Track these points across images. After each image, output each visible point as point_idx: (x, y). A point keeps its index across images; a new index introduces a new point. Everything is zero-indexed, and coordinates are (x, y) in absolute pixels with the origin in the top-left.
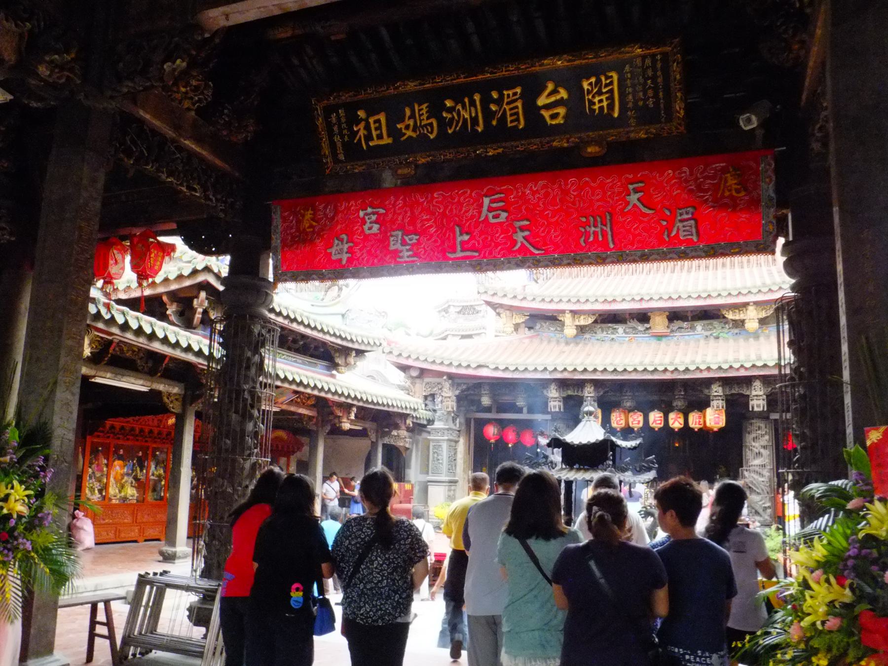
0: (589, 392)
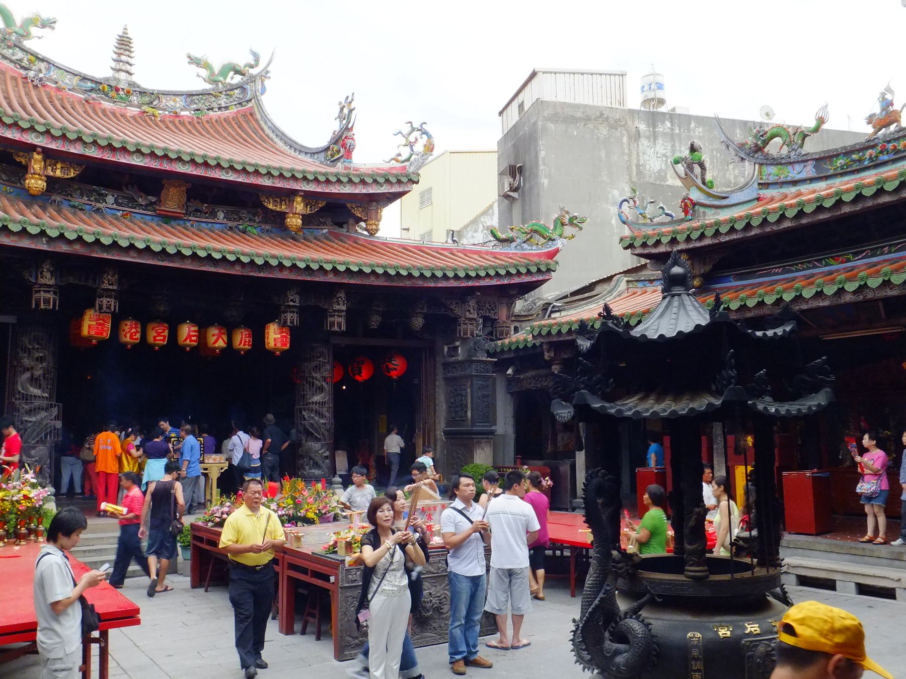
0: (109, 282)
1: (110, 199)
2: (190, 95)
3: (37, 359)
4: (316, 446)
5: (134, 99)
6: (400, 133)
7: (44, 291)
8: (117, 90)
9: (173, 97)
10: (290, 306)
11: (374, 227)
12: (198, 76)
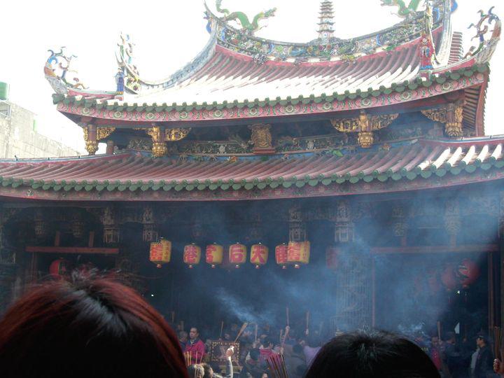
1: (222, 149)
2: (381, 34)
6: (472, 25)
8: (320, 48)
9: (368, 40)
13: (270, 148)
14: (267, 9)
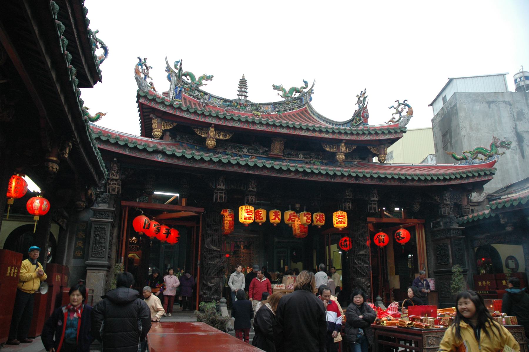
0: (252, 187)
1: (245, 150)
3: (215, 230)
4: (363, 280)
5: (249, 108)
6: (393, 107)
7: (220, 193)
8: (240, 104)
10: (347, 199)
11: (383, 158)
12: (278, 95)
13: (280, 154)
14: (208, 75)
